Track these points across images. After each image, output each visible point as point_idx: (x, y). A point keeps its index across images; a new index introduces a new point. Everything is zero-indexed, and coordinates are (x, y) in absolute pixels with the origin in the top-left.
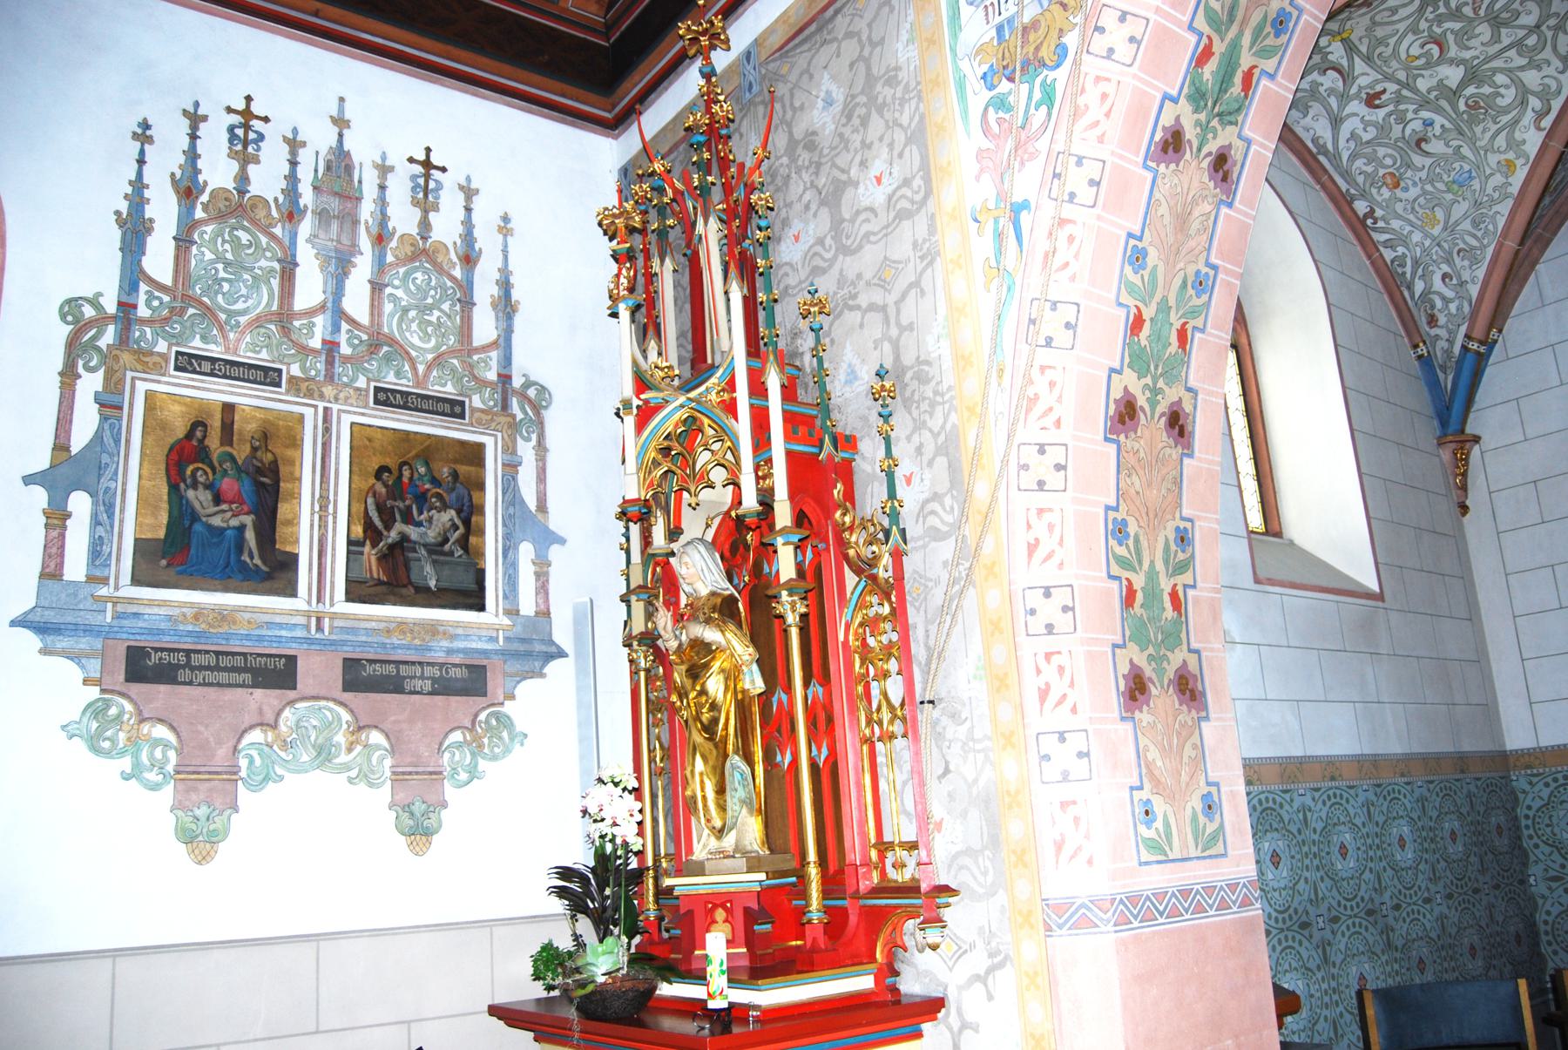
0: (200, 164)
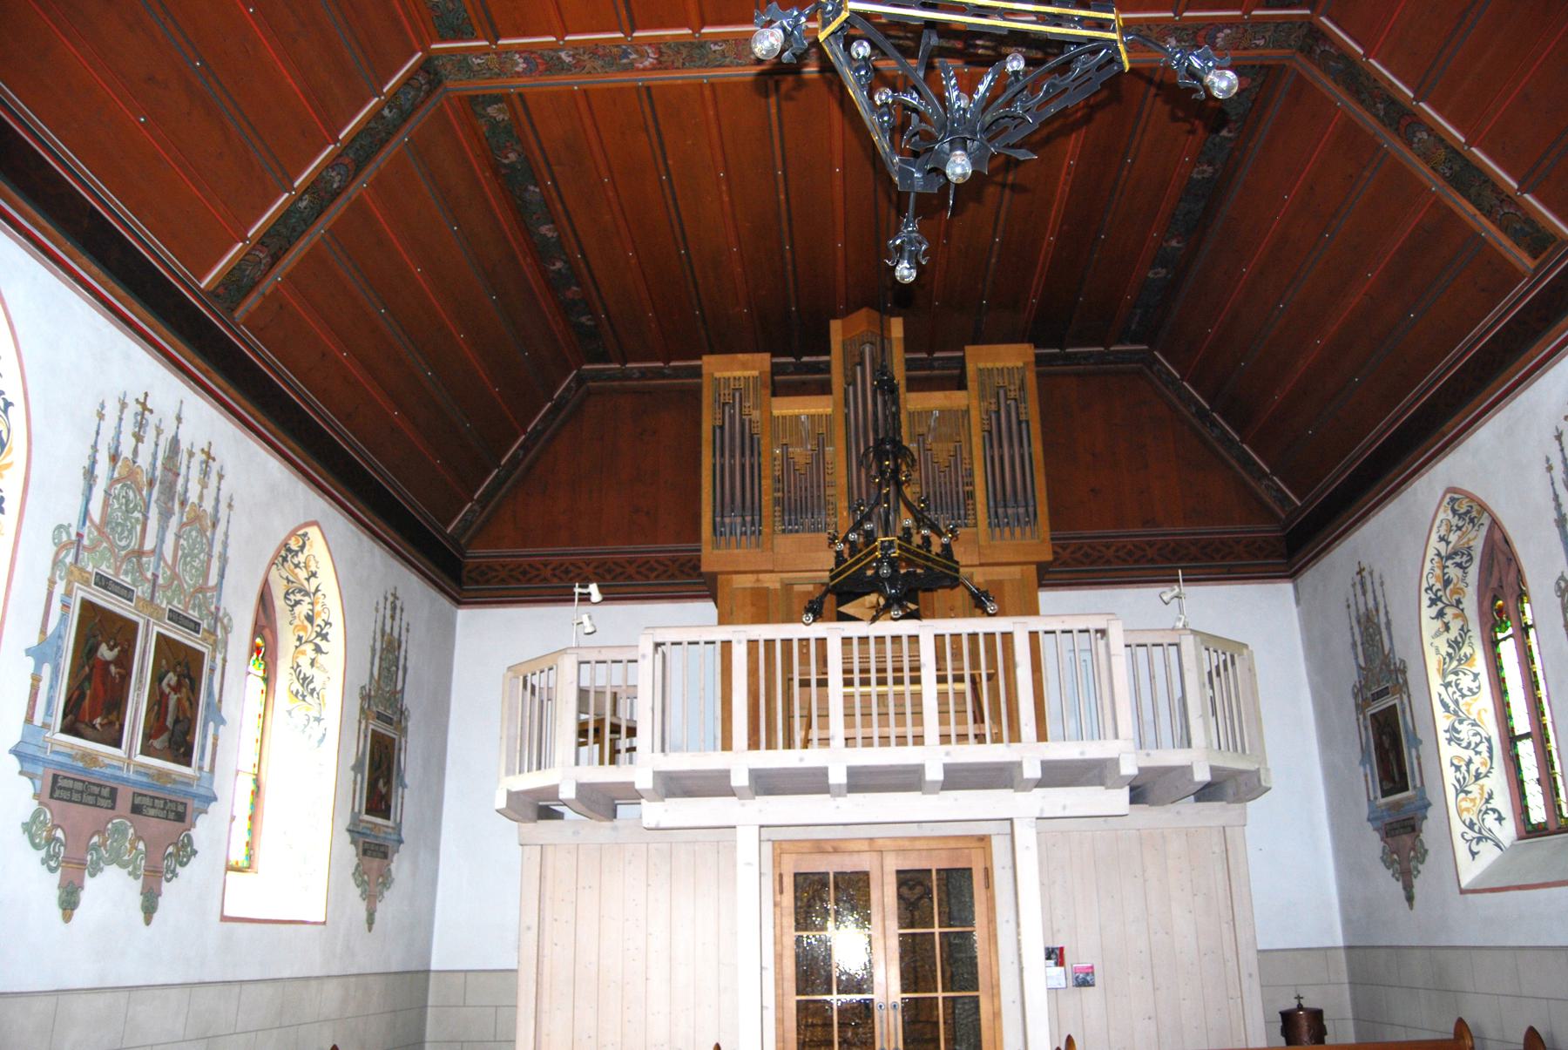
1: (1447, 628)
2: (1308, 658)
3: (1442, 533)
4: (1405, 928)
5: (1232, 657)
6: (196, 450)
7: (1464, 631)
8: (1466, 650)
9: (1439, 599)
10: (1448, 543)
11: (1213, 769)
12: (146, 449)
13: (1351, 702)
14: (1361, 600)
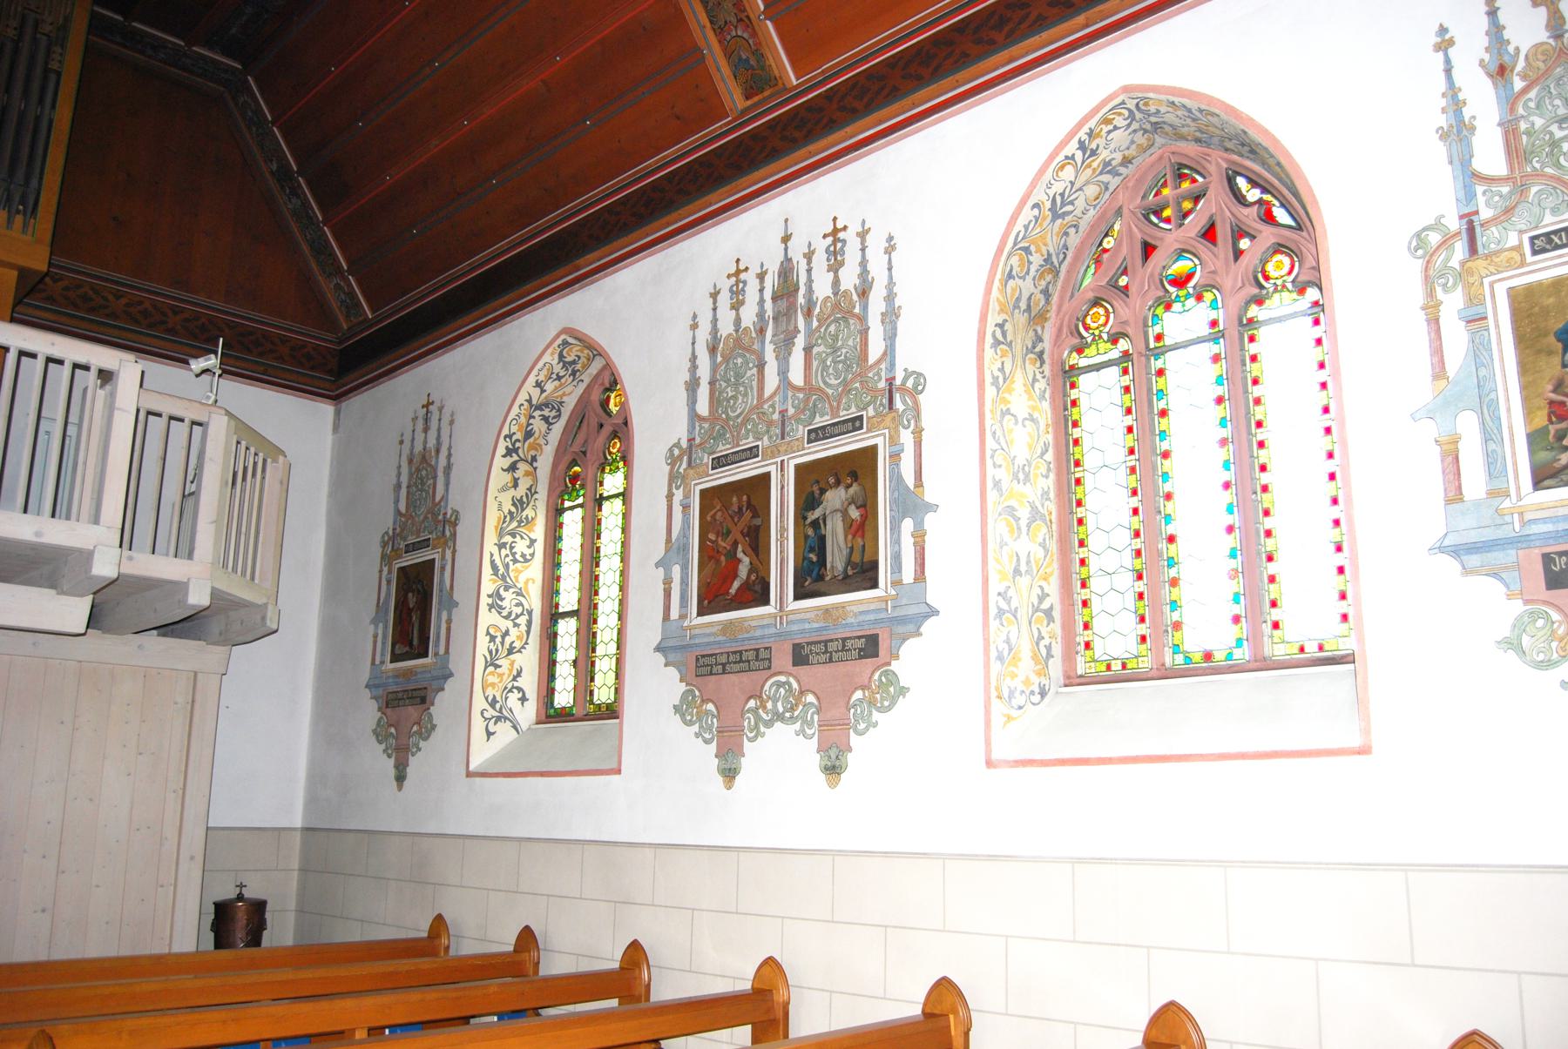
0: (1506, 34)
1: (516, 486)
2: (331, 495)
3: (541, 378)
4: (387, 809)
5: (265, 461)
7: (531, 491)
8: (529, 512)
9: (516, 451)
10: (543, 391)
11: (215, 594)
13: (376, 551)
14: (420, 437)
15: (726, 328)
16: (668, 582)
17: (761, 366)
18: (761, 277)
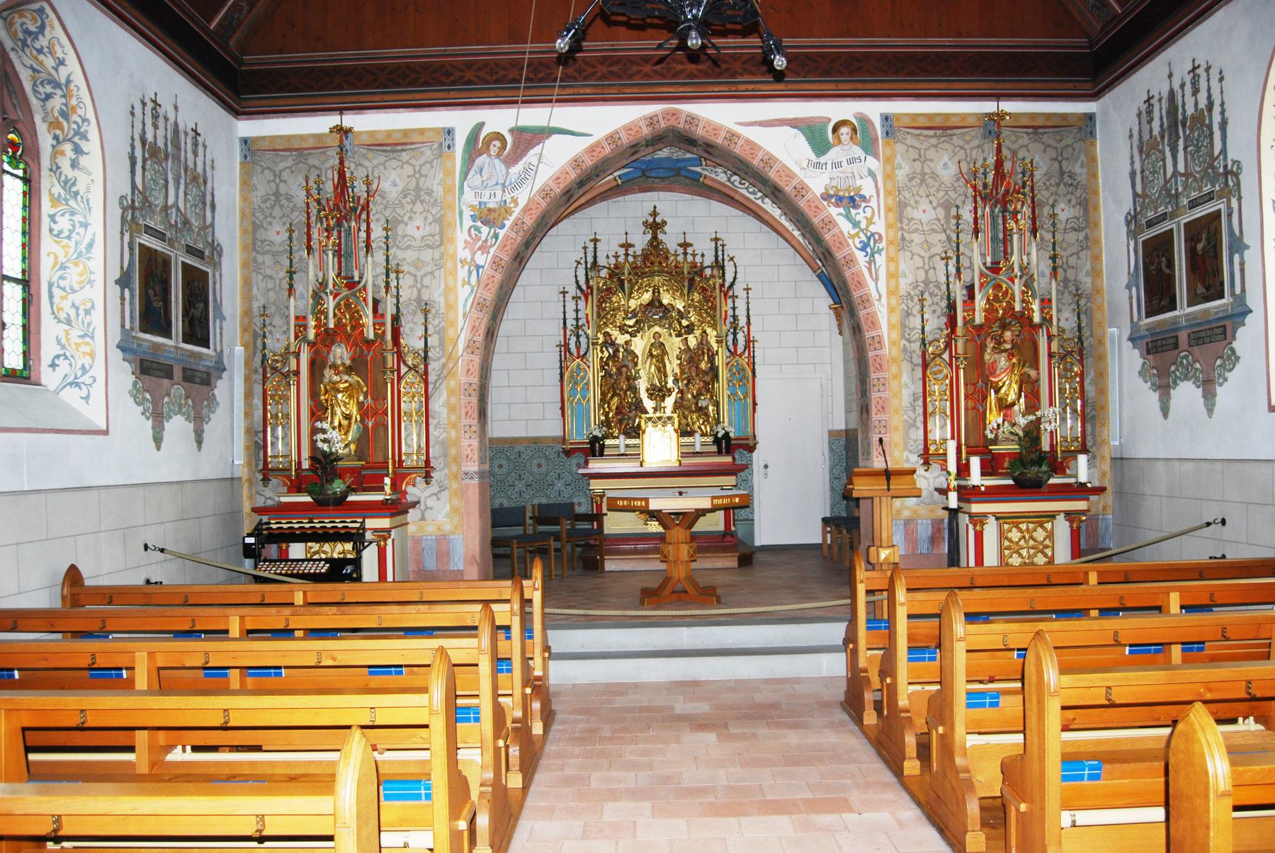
6: (189, 130)
12: (161, 132)
15: (1146, 137)
16: (1131, 298)
17: (1164, 160)
18: (1160, 100)
